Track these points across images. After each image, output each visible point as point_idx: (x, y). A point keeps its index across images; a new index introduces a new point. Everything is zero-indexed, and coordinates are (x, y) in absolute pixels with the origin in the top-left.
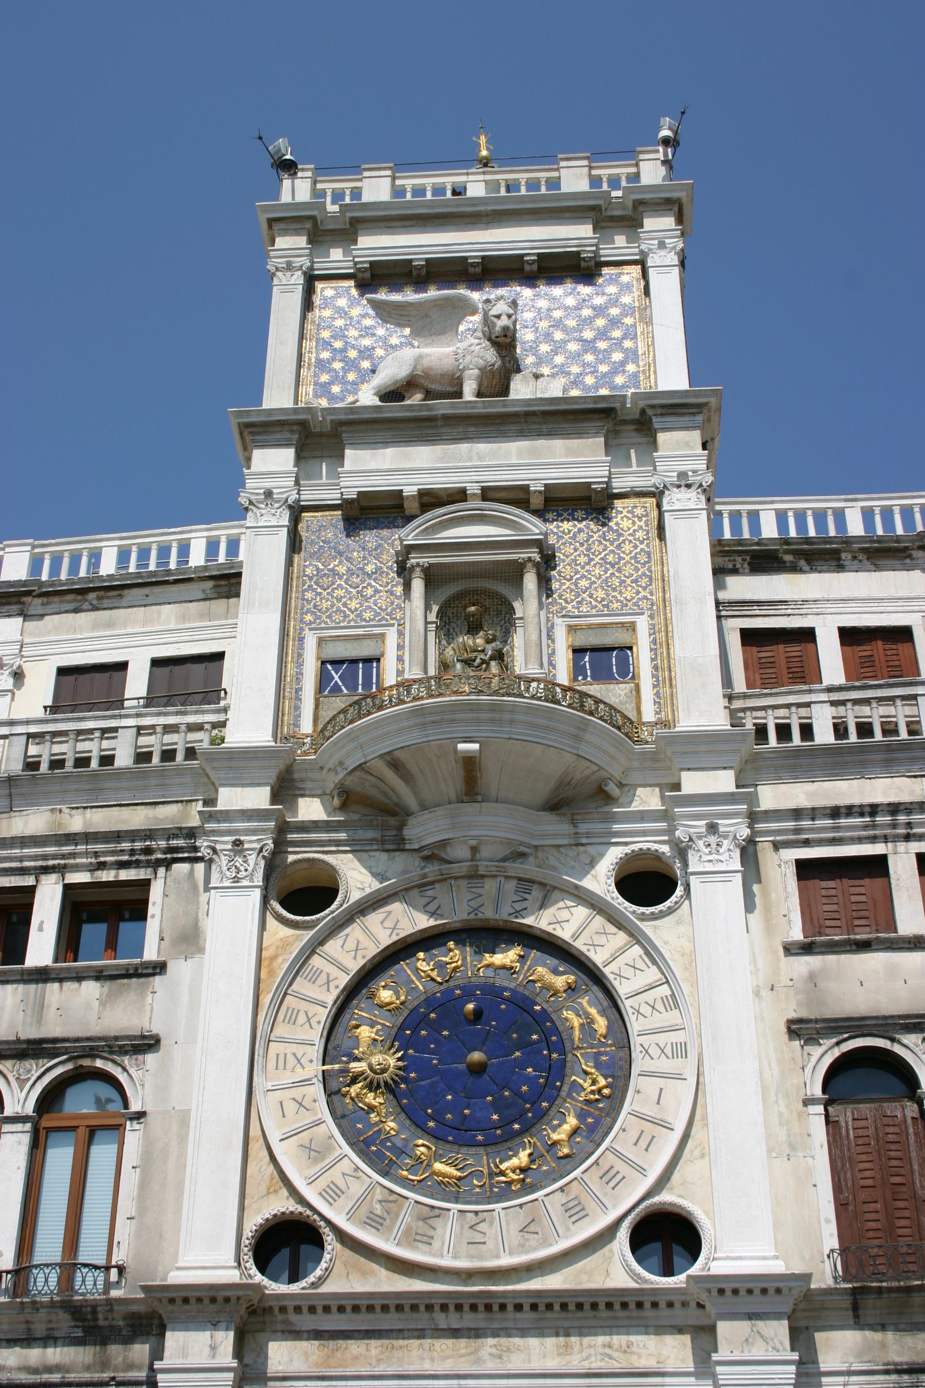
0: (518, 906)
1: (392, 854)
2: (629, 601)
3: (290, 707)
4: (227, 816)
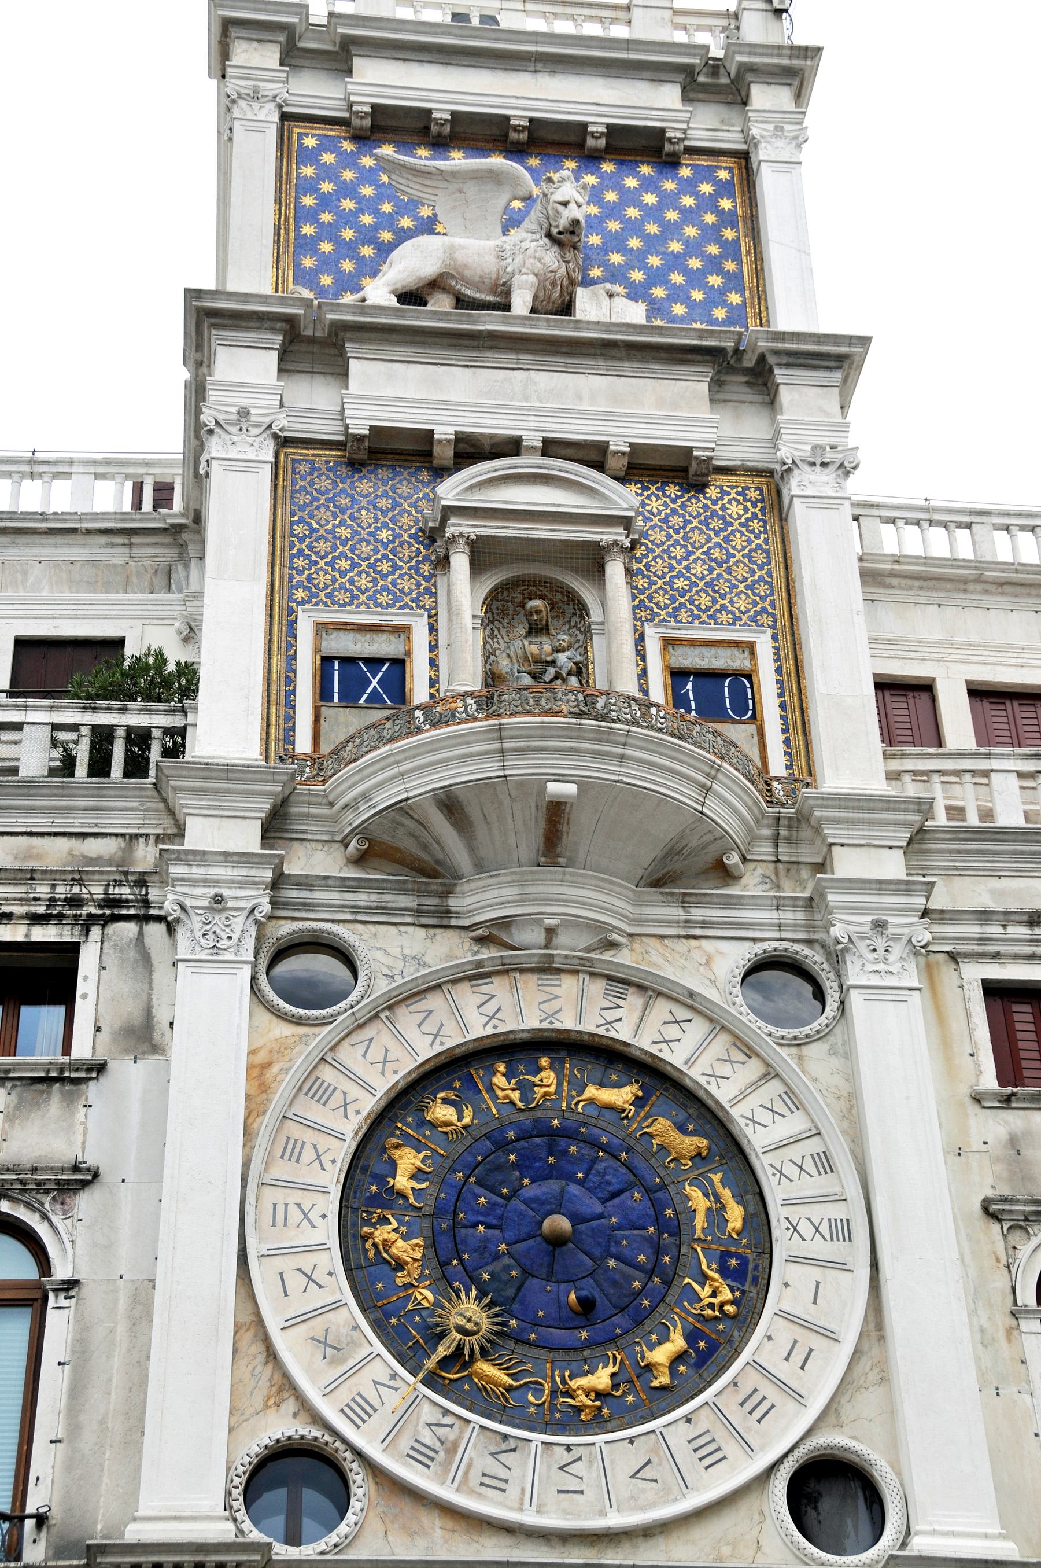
0: (611, 1015)
1: (432, 931)
3: (278, 717)
4: (202, 857)
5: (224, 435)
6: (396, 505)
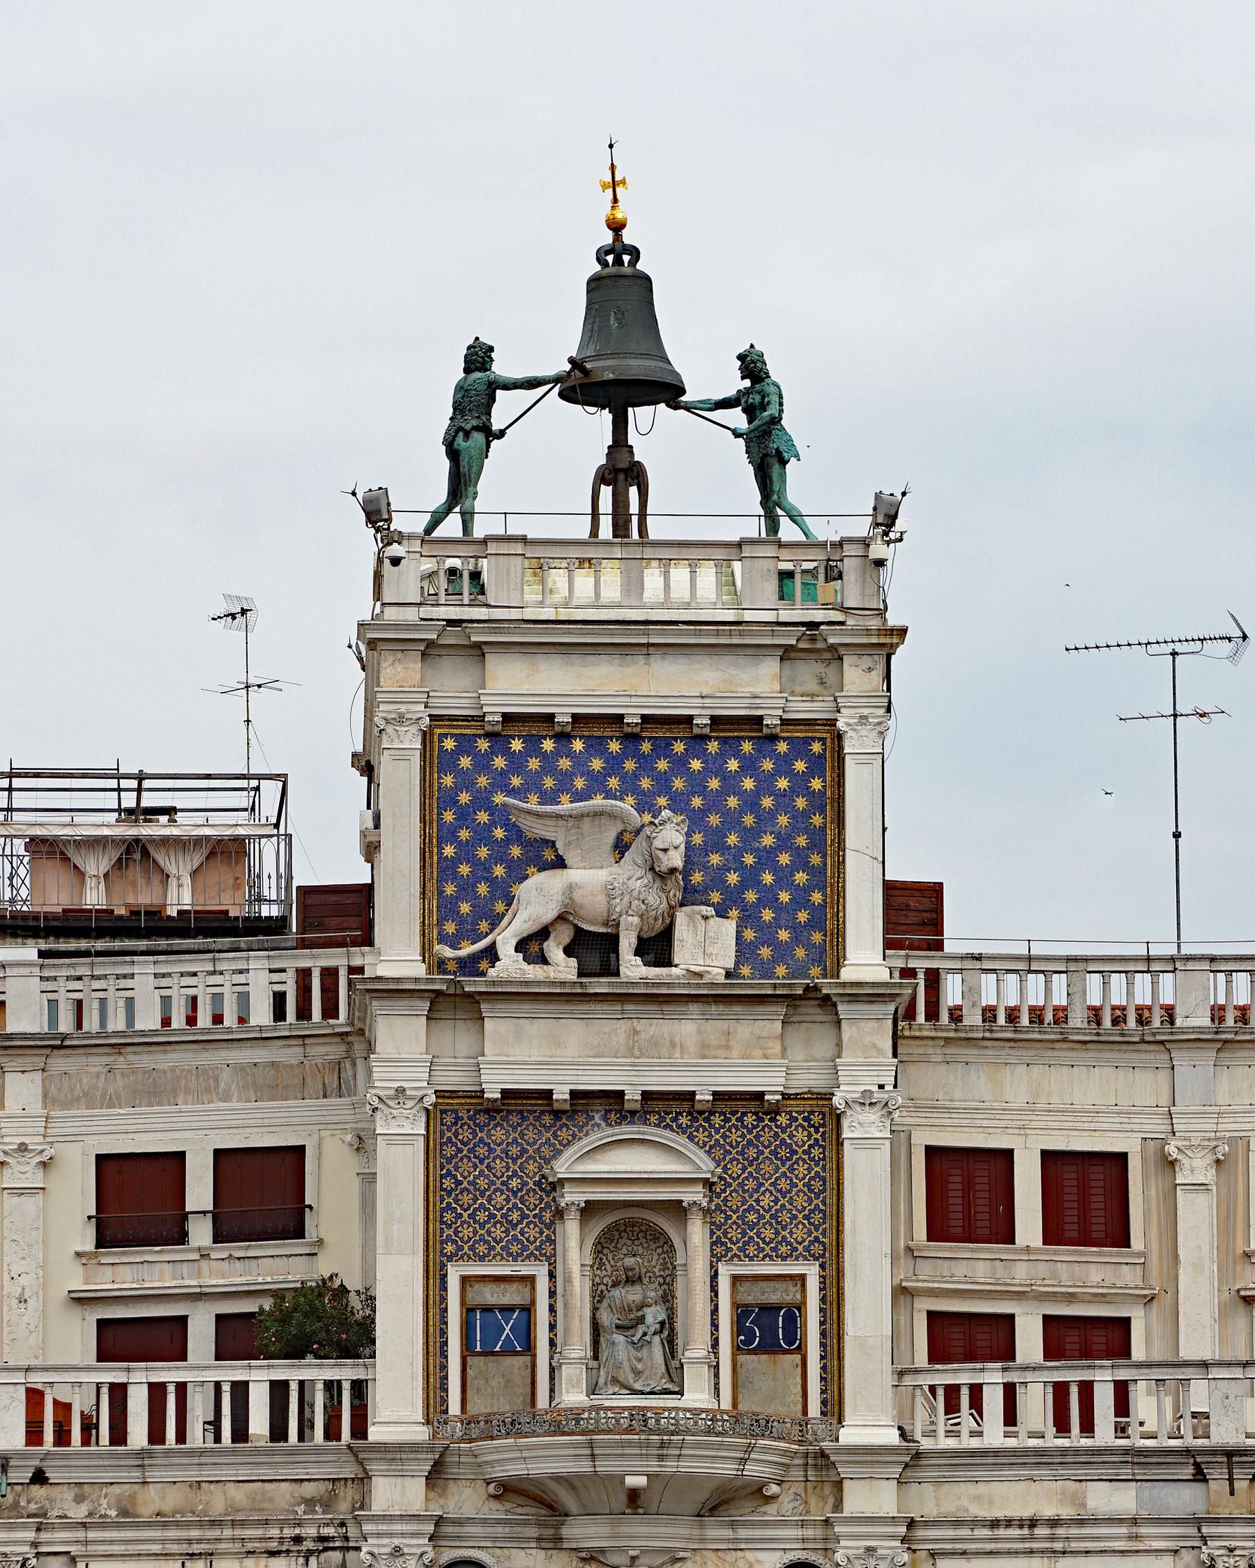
1: (550, 1552)
2: (800, 1244)
5: (387, 1111)
6: (524, 1151)
